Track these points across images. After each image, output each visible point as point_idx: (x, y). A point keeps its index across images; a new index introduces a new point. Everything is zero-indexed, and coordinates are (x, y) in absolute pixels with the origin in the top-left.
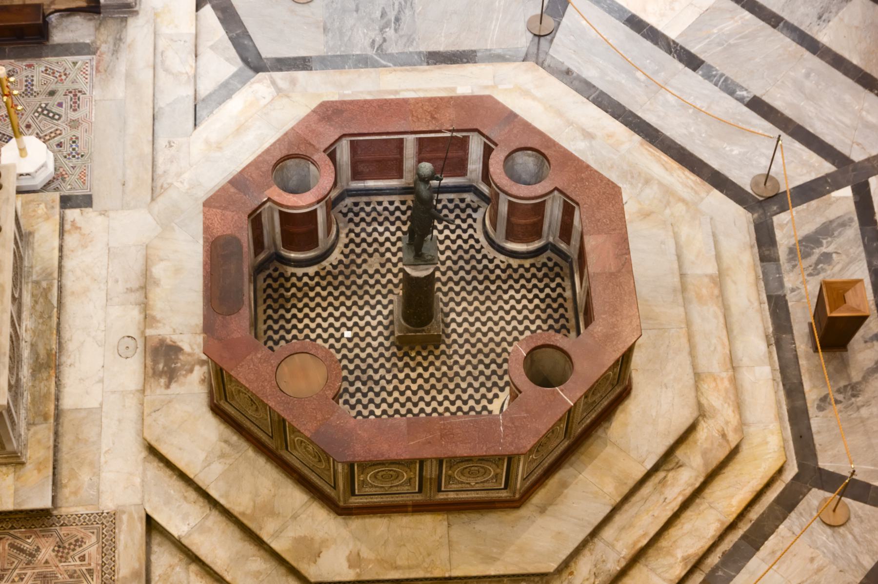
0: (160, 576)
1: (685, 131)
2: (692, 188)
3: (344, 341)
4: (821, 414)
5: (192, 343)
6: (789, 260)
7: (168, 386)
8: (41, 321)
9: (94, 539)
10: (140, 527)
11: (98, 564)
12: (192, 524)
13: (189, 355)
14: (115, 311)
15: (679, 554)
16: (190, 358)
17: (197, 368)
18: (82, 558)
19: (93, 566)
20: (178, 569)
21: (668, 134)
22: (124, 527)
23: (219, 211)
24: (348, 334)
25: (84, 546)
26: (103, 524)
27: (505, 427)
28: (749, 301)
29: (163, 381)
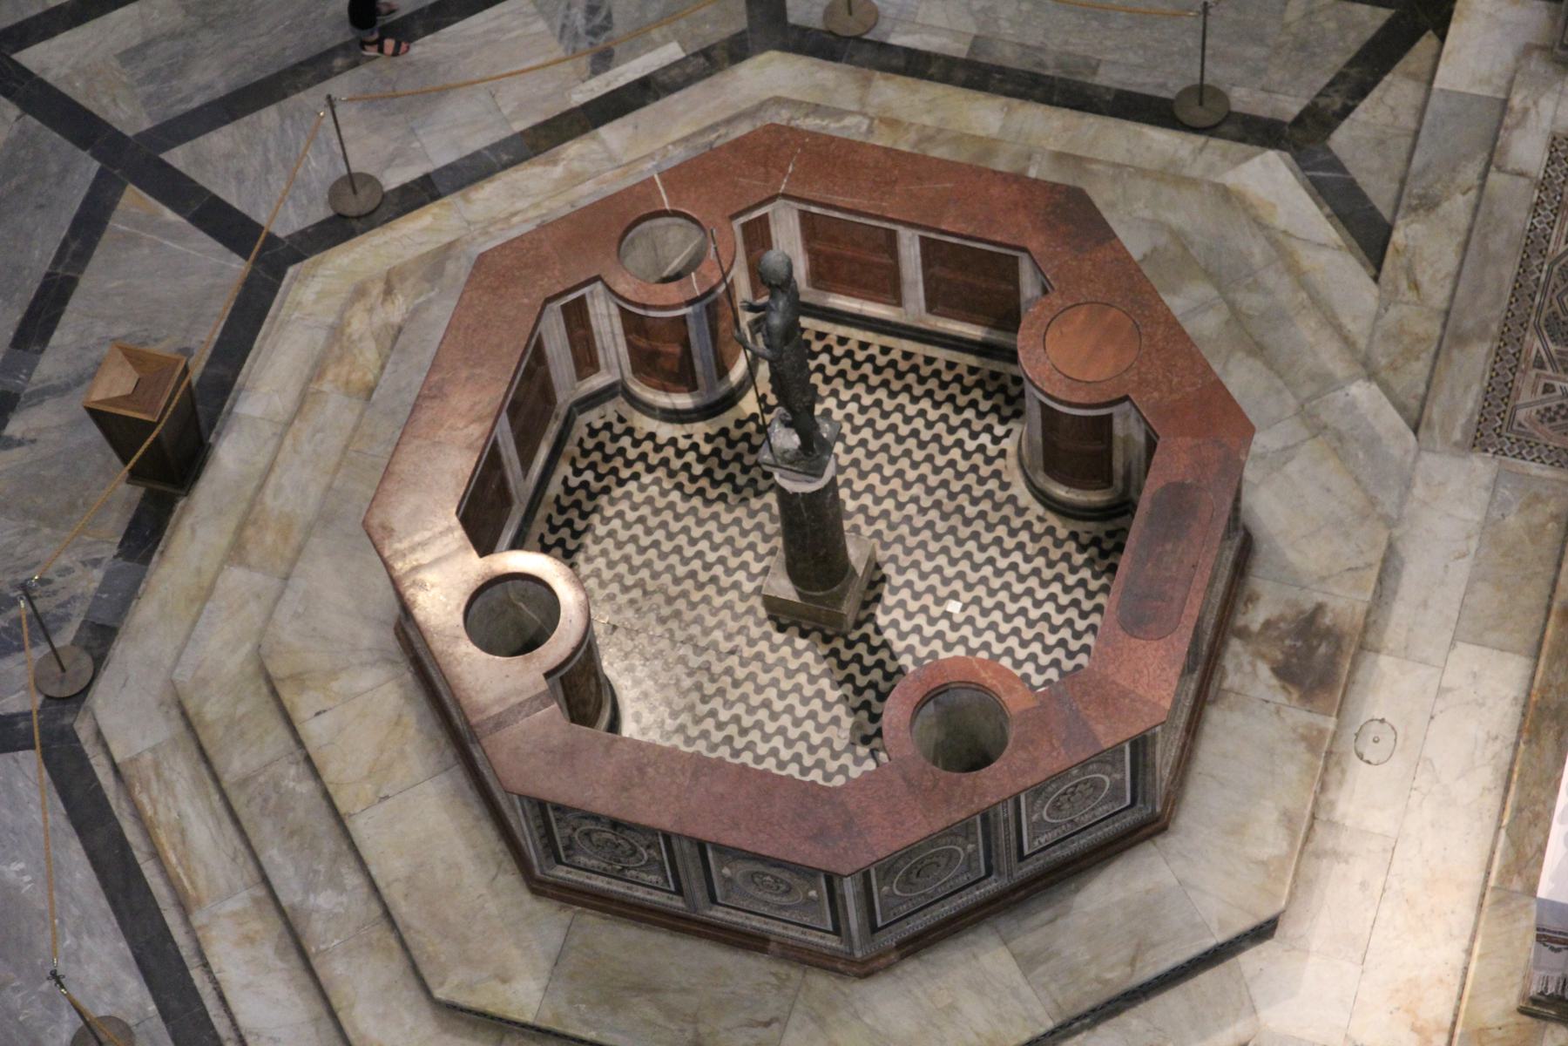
0: (1418, 359)
1: (87, 942)
2: (159, 776)
3: (966, 597)
4: (193, 343)
5: (1249, 673)
6: (66, 618)
7: (1320, 608)
8: (1539, 808)
9: (1521, 415)
10: (1435, 412)
11: (1524, 372)
12: (1338, 393)
13: (1263, 657)
14: (1380, 822)
15: (558, 171)
16: (1264, 649)
17: (1256, 627)
18: (1548, 389)
19: (1533, 373)
20: (1384, 362)
21: (123, 944)
22: (1462, 420)
23: (1141, 691)
24: (954, 607)
25: (1541, 407)
26: (1499, 435)
27: (783, 171)
28: (193, 531)
29: (1327, 620)
